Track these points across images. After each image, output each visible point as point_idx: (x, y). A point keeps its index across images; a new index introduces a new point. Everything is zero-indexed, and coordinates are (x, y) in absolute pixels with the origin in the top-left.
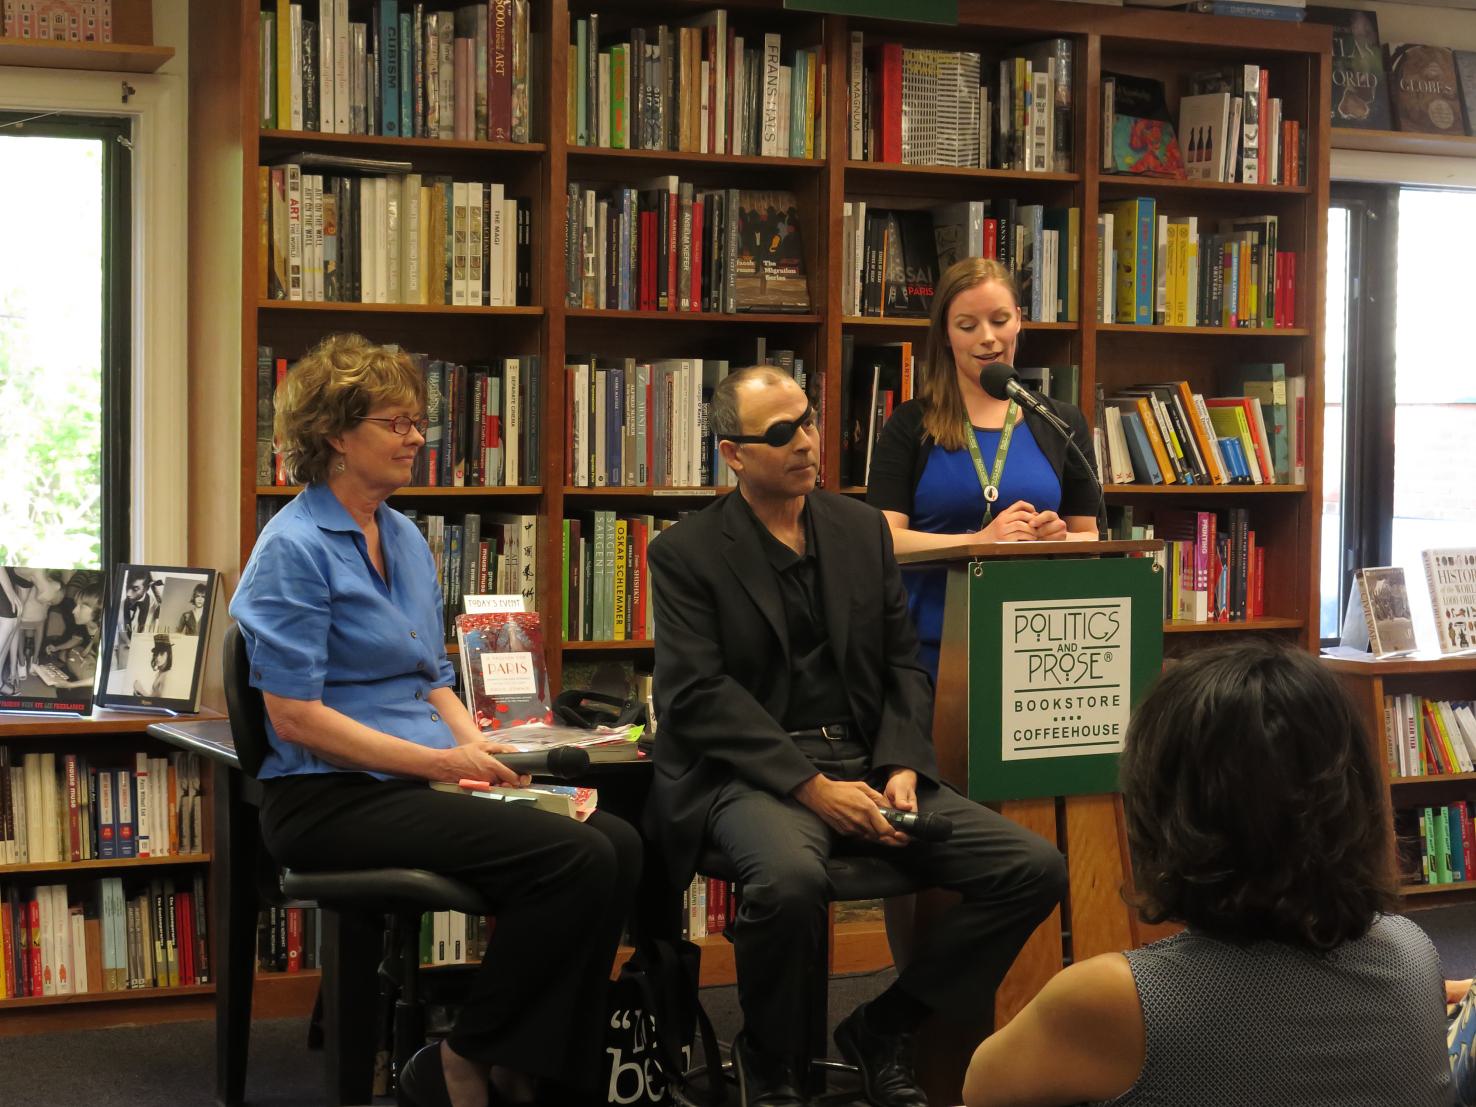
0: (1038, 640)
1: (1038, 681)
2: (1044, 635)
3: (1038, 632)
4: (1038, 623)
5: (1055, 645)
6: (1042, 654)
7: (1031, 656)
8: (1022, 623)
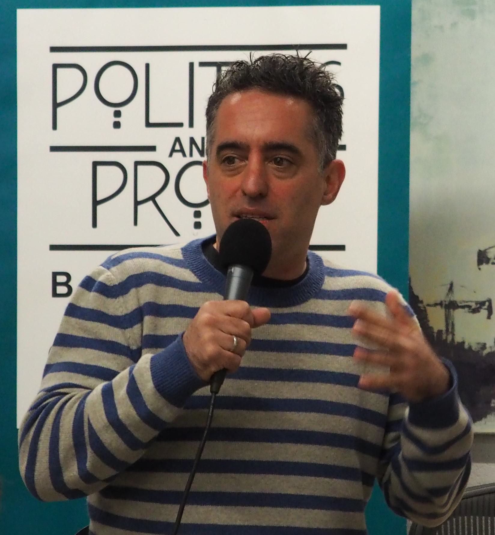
0: (117, 125)
1: (116, 222)
2: (133, 113)
3: (117, 108)
4: (117, 84)
5: (163, 139)
6: (128, 159)
7: (95, 164)
8: (69, 81)
